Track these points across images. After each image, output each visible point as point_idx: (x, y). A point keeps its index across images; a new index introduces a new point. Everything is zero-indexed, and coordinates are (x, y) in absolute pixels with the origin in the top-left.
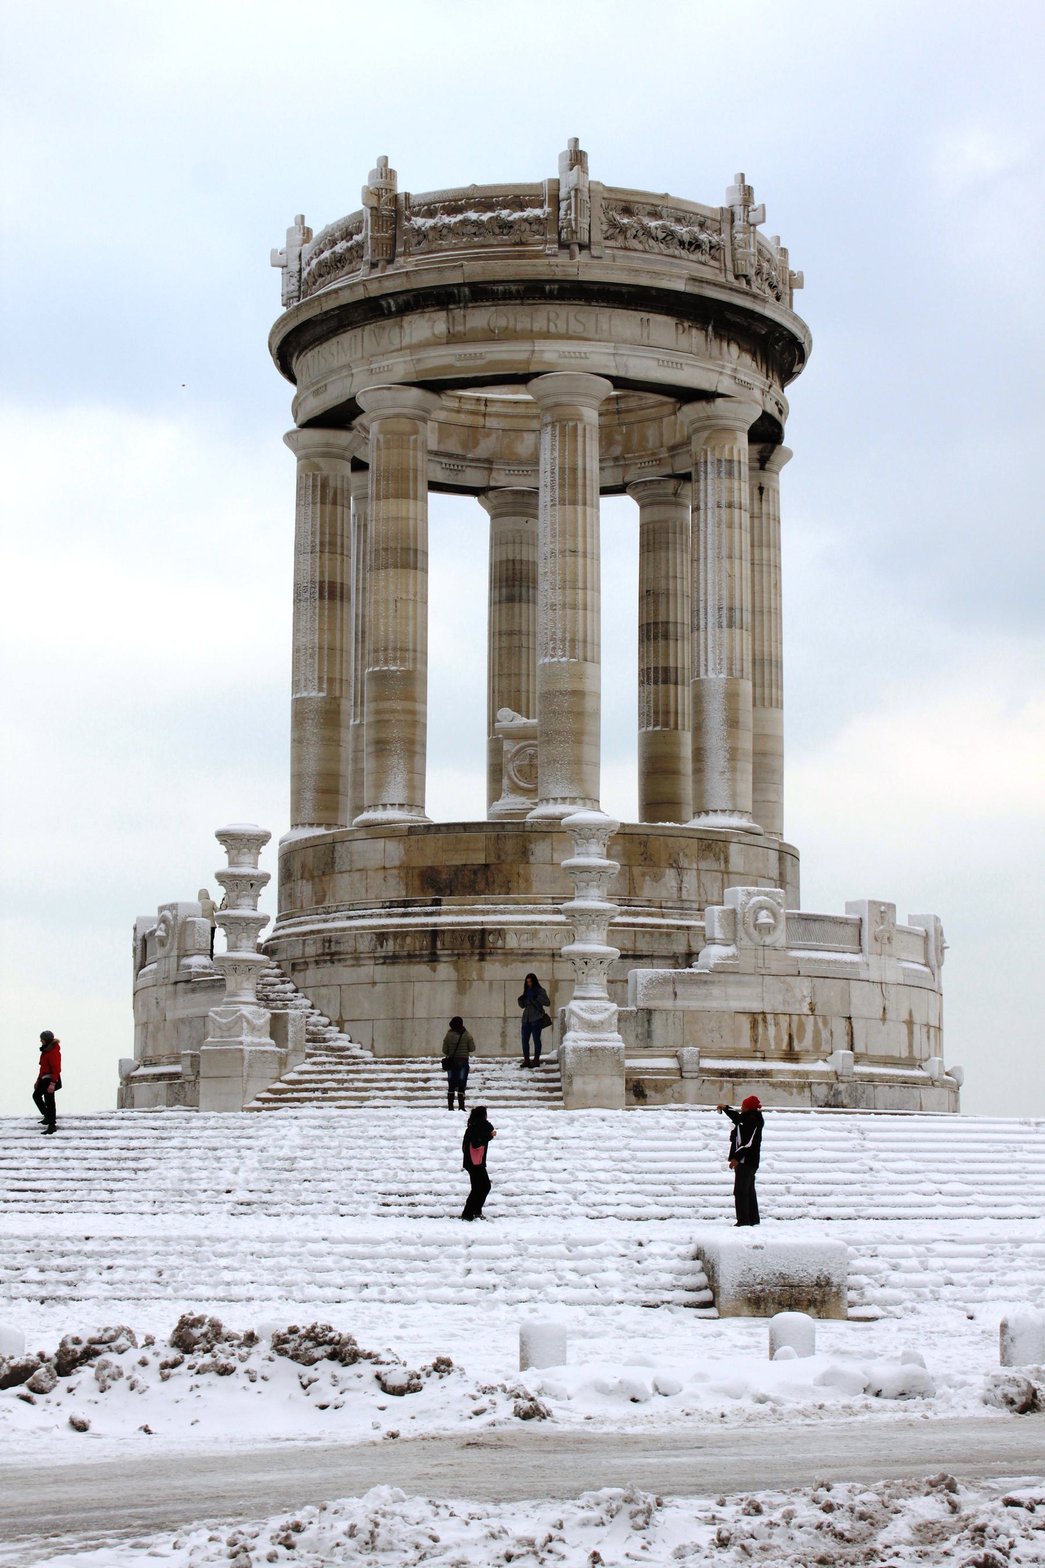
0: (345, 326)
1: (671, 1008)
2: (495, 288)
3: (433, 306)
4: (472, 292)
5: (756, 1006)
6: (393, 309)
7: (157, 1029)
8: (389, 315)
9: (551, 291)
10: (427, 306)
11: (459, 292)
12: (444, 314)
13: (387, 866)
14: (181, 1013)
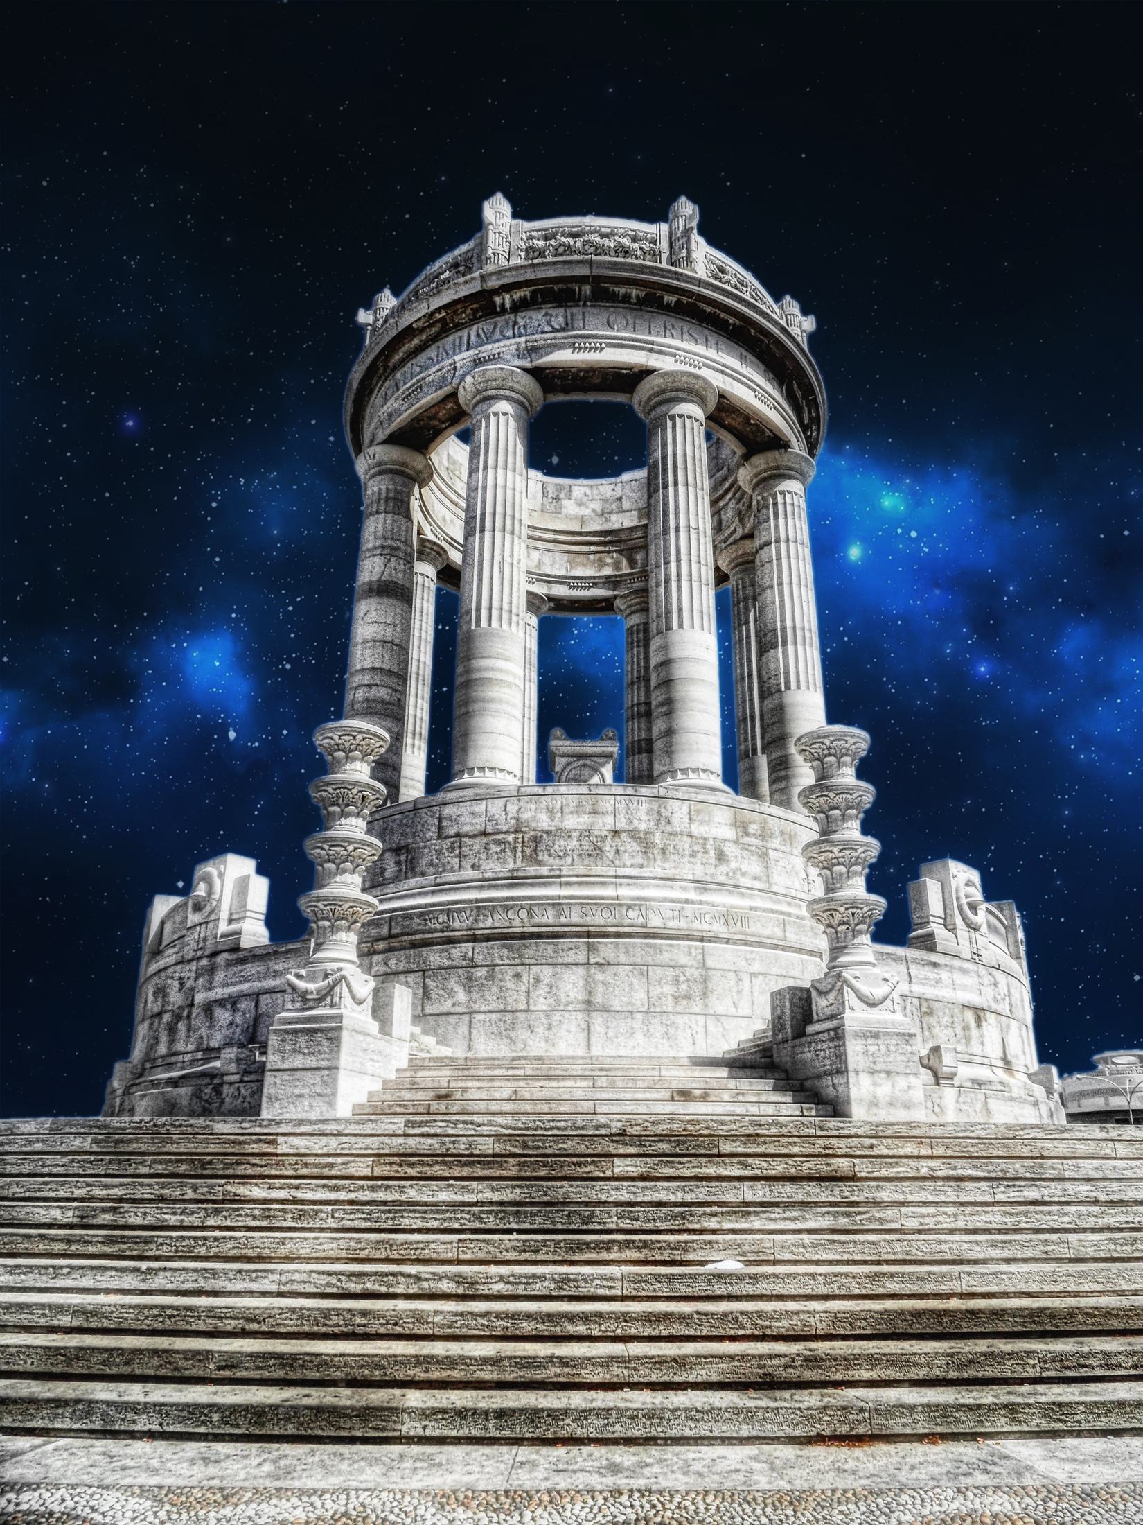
0: (449, 329)
1: (908, 994)
2: (616, 289)
3: (550, 302)
4: (592, 291)
5: (976, 1000)
6: (508, 306)
7: (178, 1017)
8: (504, 311)
9: (669, 304)
10: (544, 302)
11: (580, 290)
12: (562, 310)
13: (489, 829)
14: (218, 993)
